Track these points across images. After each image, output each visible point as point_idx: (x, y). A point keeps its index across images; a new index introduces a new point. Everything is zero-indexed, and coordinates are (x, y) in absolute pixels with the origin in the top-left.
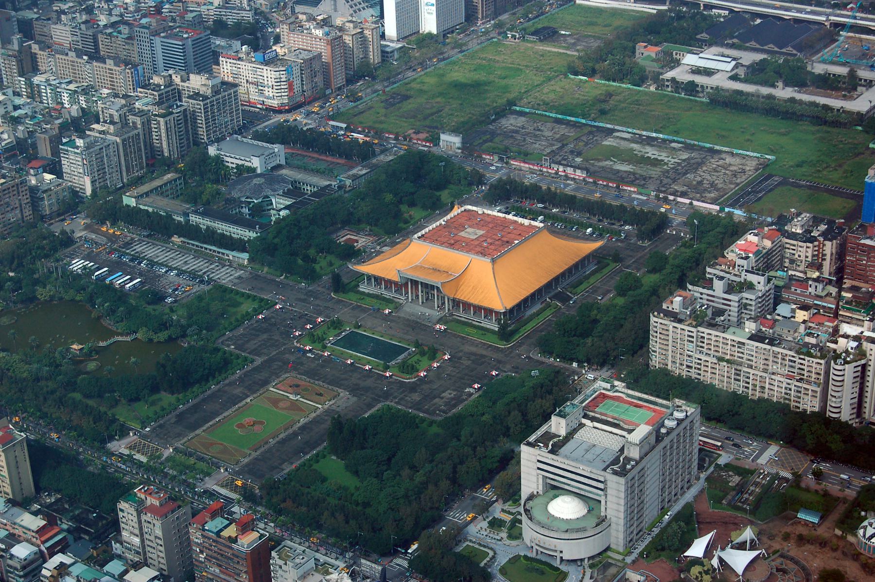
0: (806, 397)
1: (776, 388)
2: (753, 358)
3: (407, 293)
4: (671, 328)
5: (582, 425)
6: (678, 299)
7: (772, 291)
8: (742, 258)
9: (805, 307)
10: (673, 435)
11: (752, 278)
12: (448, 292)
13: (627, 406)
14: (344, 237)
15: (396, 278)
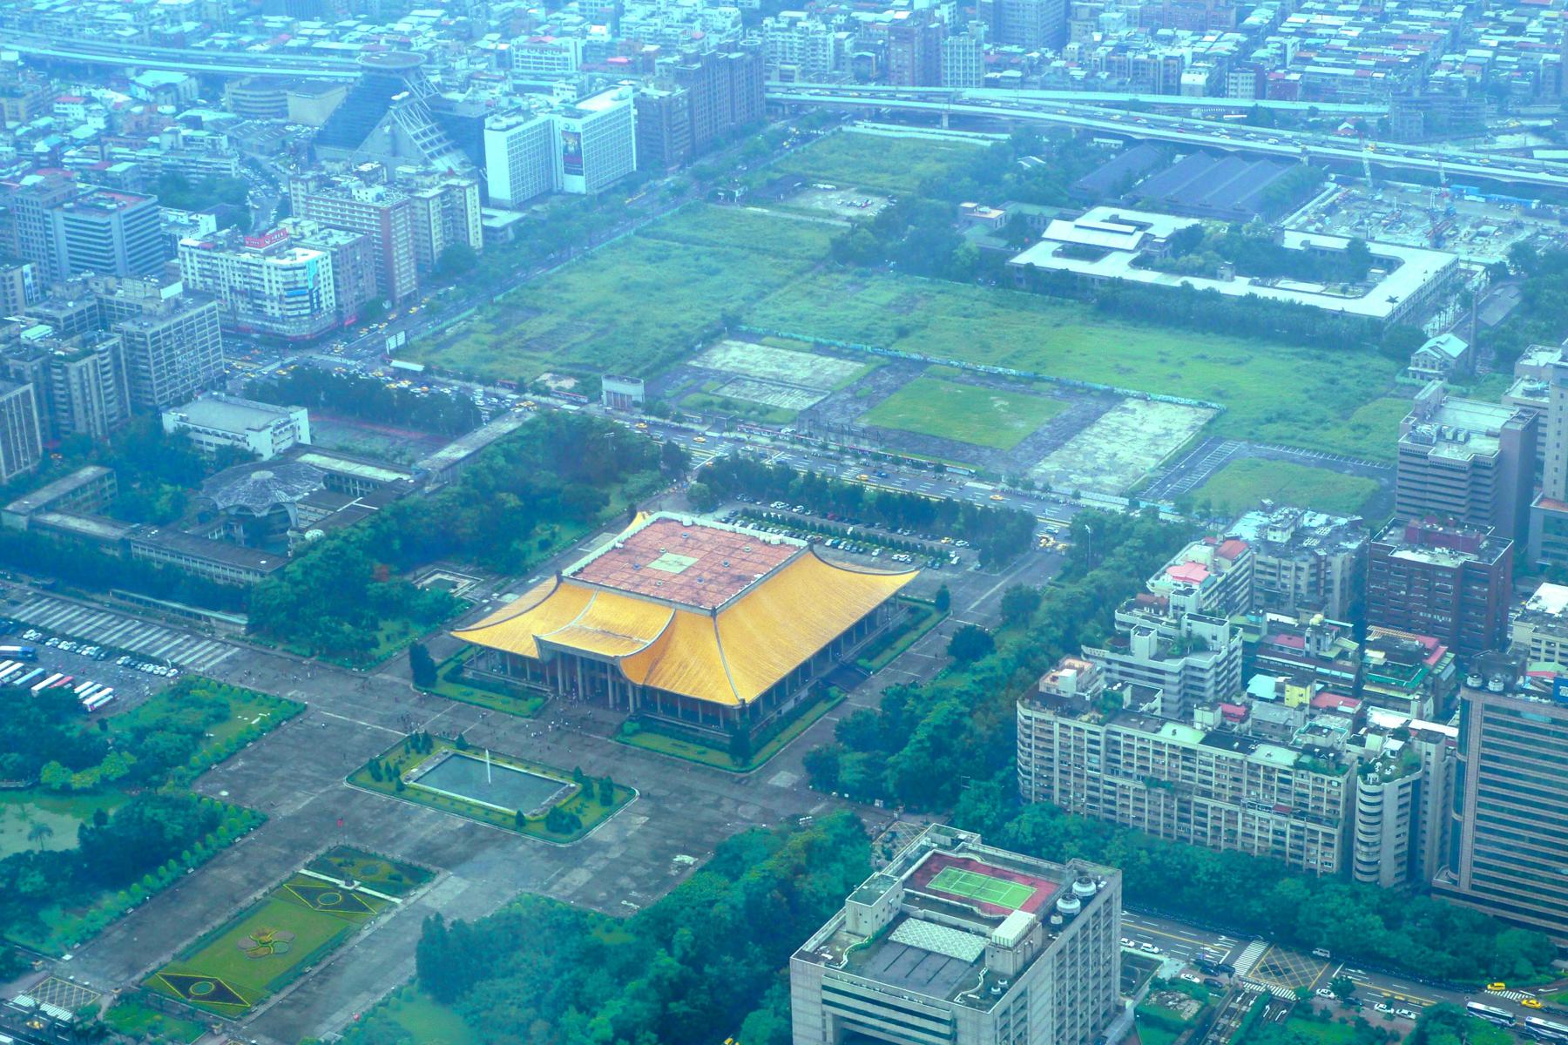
0: (1312, 846)
1: (1256, 833)
2: (1213, 779)
3: (554, 682)
4: (1056, 727)
5: (902, 917)
6: (1068, 673)
7: (1239, 653)
8: (1179, 592)
9: (1302, 679)
10: (1075, 927)
11: (1202, 629)
12: (636, 676)
13: (982, 877)
14: (430, 579)
15: (533, 653)
